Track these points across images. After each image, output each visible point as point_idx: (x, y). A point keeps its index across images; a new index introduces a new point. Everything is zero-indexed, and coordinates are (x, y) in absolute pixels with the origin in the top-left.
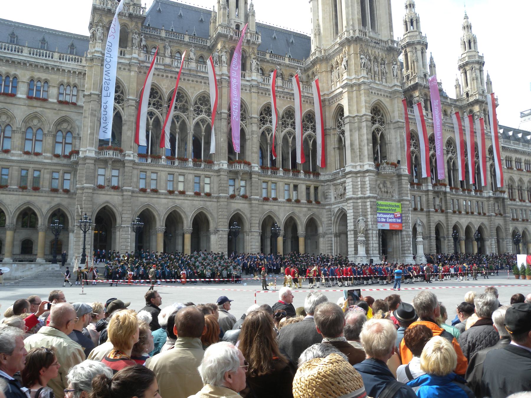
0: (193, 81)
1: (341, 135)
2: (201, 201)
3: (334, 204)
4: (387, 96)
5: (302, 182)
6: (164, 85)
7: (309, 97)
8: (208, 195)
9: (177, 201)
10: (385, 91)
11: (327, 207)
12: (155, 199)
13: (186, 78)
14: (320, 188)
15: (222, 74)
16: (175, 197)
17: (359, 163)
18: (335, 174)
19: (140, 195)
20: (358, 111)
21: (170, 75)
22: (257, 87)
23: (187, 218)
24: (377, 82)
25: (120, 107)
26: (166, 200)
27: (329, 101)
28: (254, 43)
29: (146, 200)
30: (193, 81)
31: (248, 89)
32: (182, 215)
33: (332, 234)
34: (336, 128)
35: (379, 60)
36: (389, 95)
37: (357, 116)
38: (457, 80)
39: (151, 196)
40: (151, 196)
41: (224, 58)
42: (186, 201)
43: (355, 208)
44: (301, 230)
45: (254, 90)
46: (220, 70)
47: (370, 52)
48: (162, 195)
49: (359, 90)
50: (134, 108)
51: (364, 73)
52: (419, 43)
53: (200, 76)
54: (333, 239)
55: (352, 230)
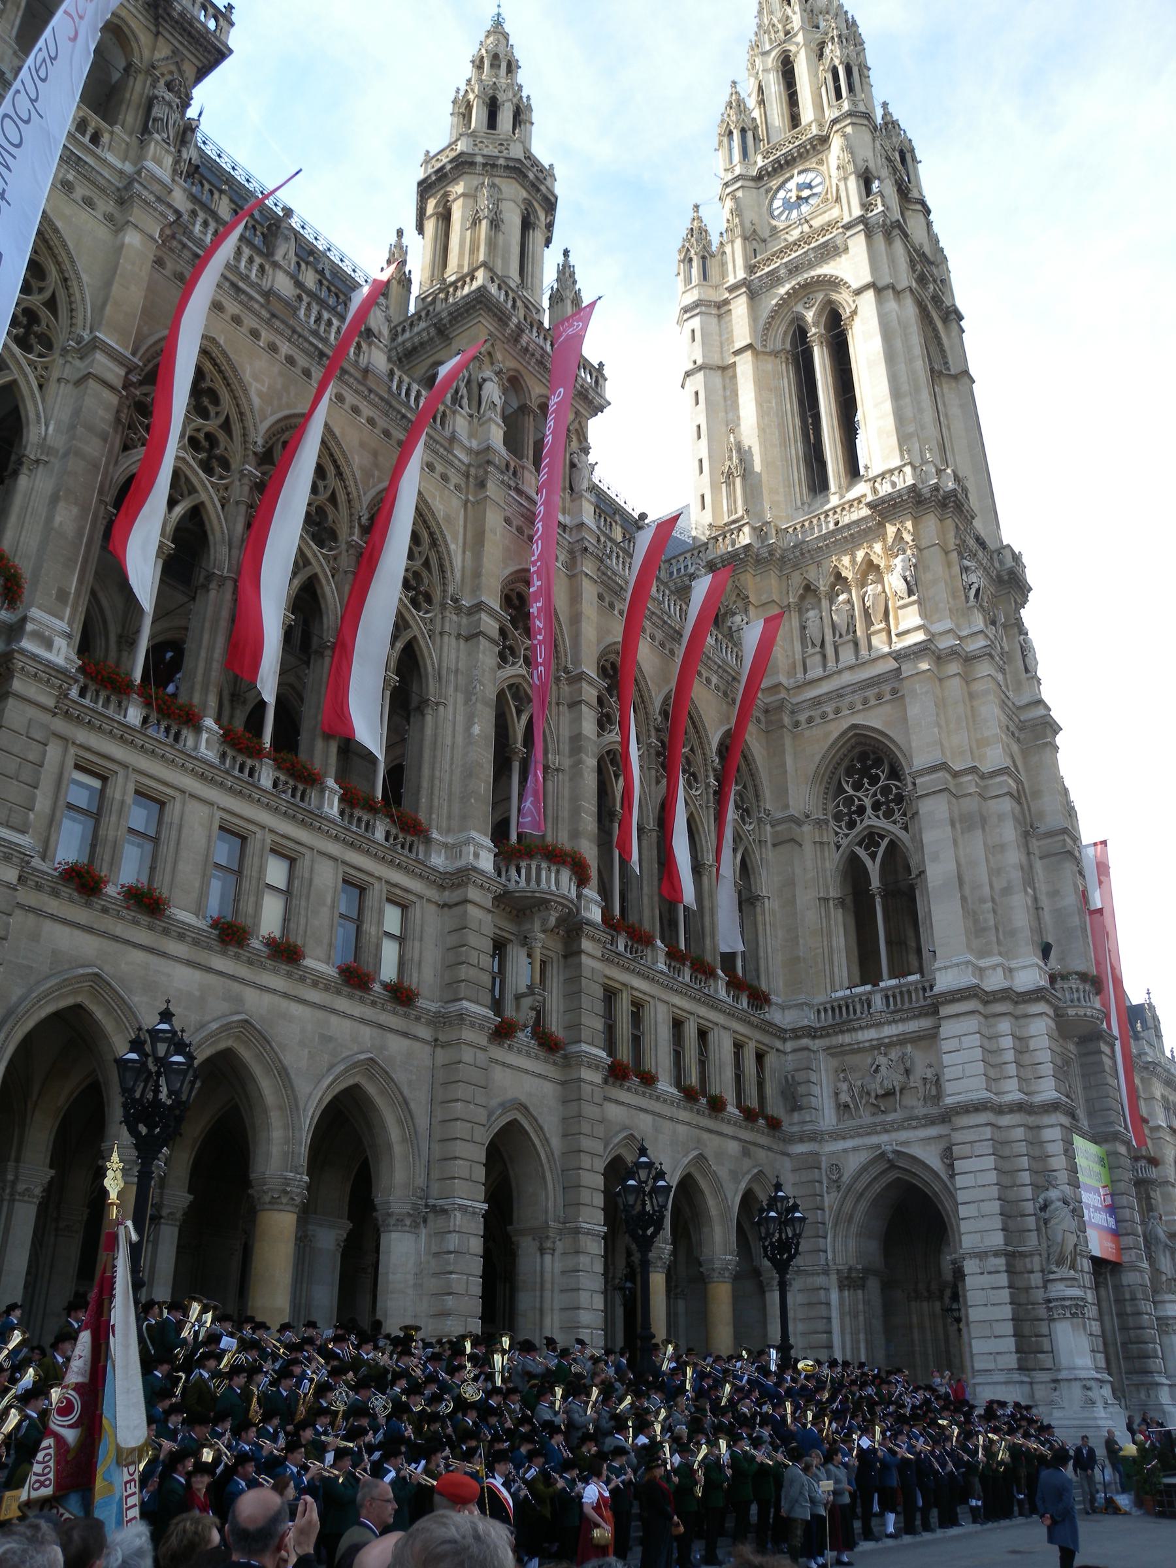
0: (371, 421)
1: (861, 853)
2: (363, 1021)
3: (836, 1136)
5: (720, 1018)
6: (256, 379)
8: (401, 996)
9: (251, 996)
11: (799, 1148)
12: (139, 956)
14: (771, 1060)
16: (242, 971)
17: (997, 959)
18: (835, 1008)
19: (53, 905)
21: (285, 348)
23: (292, 1106)
25: (28, 370)
26: (197, 975)
27: (793, 712)
29: (87, 946)
30: (371, 421)
32: (266, 1085)
33: (826, 1273)
34: (826, 822)
37: (974, 770)
39: (119, 929)
40: (119, 929)
42: (296, 1009)
43: (1000, 1149)
44: (720, 1243)
48: (181, 937)
49: (967, 679)
50: (114, 400)
54: (834, 1296)
55: (996, 1254)
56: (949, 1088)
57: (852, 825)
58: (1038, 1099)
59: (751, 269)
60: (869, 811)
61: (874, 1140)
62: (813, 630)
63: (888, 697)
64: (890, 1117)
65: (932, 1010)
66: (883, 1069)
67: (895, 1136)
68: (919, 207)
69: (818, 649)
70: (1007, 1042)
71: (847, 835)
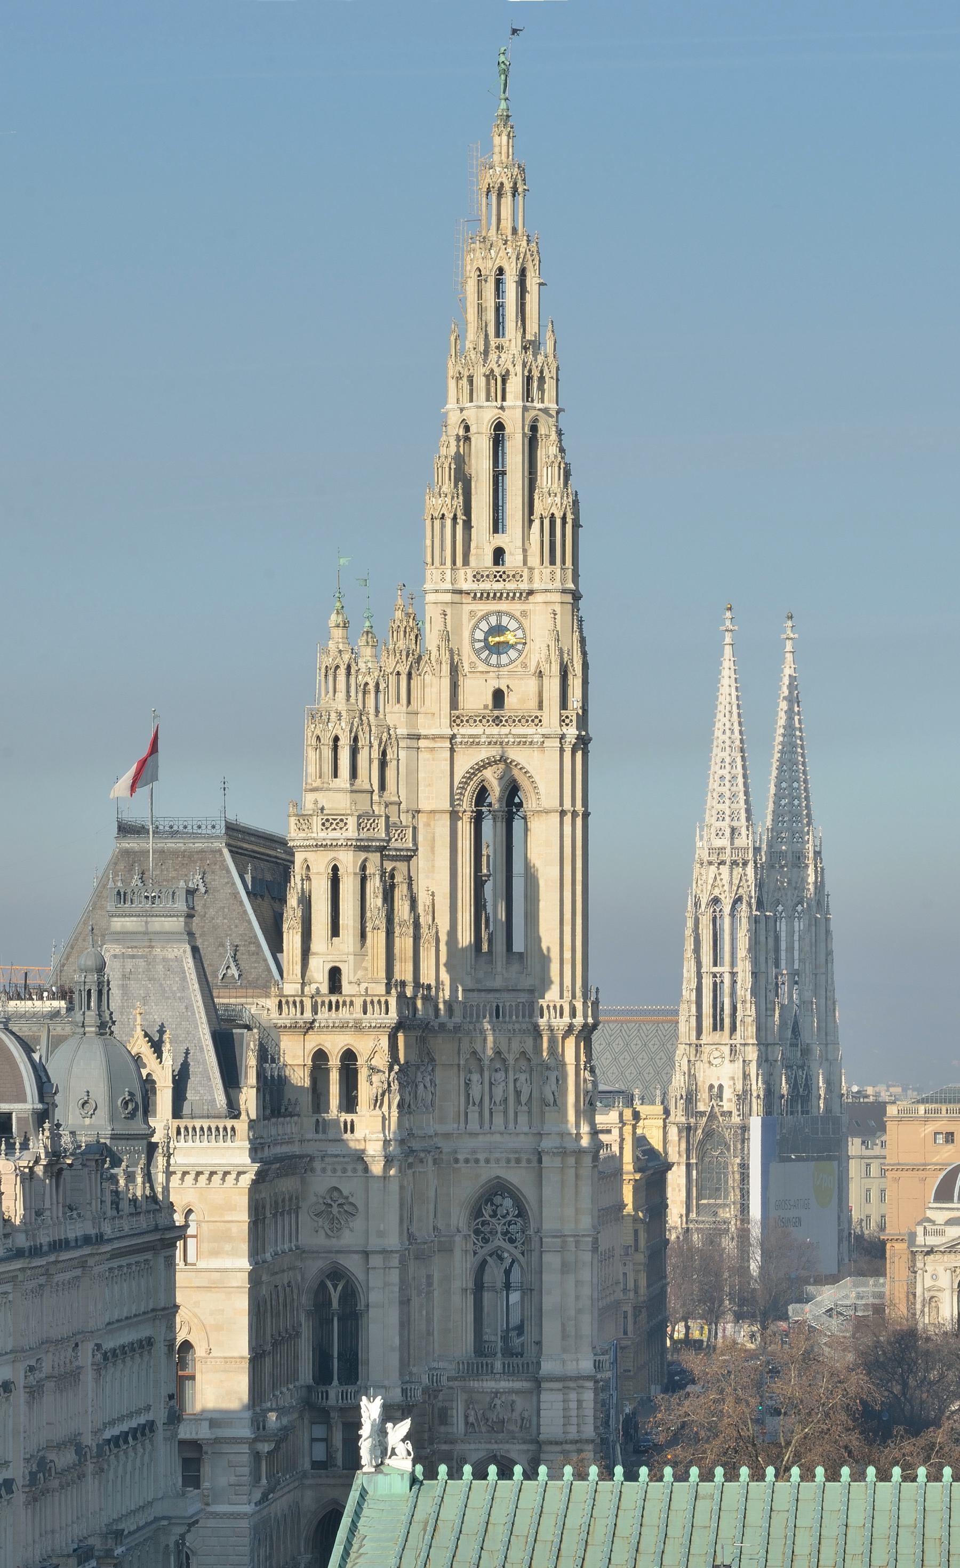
34: (469, 1235)
56: (542, 1429)
57: (486, 1241)
58: (584, 1436)
59: (455, 720)
60: (499, 1235)
61: (489, 1446)
62: (475, 1092)
63: (524, 1164)
64: (500, 1436)
65: (538, 1382)
66: (498, 1406)
67: (501, 1446)
69: (476, 1108)
70: (573, 1405)
71: (482, 1247)
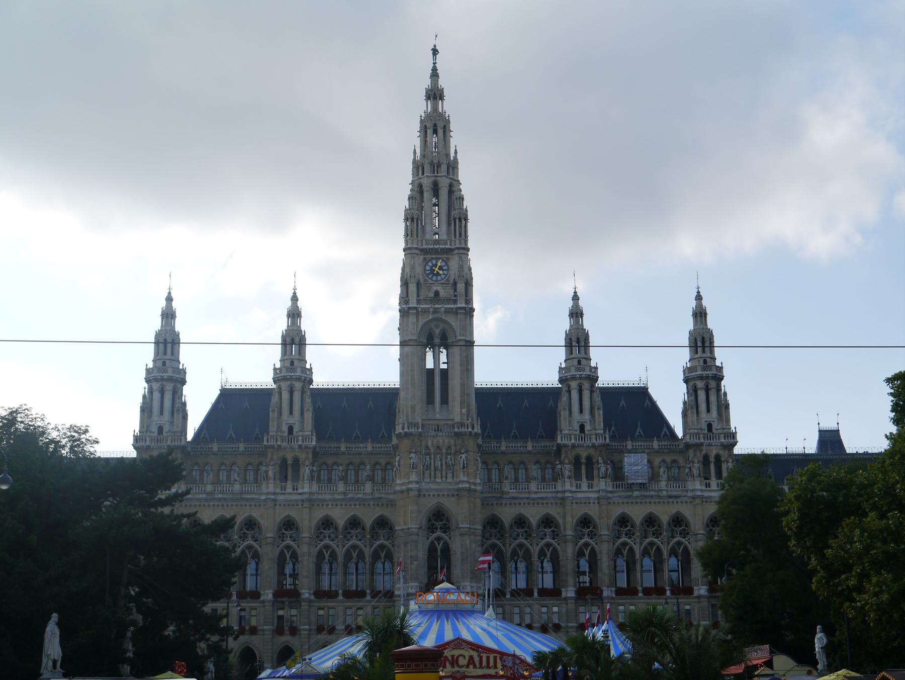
4: (453, 495)
7: (379, 498)
10: (450, 490)
13: (230, 504)
15: (268, 494)
20: (405, 523)
21: (212, 504)
22: (310, 500)
24: (439, 480)
28: (306, 447)
31: (300, 503)
35: (444, 451)
36: (455, 493)
38: (685, 403)
41: (271, 474)
45: (306, 504)
46: (268, 488)
47: (430, 444)
51: (414, 477)
52: (574, 378)
53: (243, 499)
68: (456, 251)
